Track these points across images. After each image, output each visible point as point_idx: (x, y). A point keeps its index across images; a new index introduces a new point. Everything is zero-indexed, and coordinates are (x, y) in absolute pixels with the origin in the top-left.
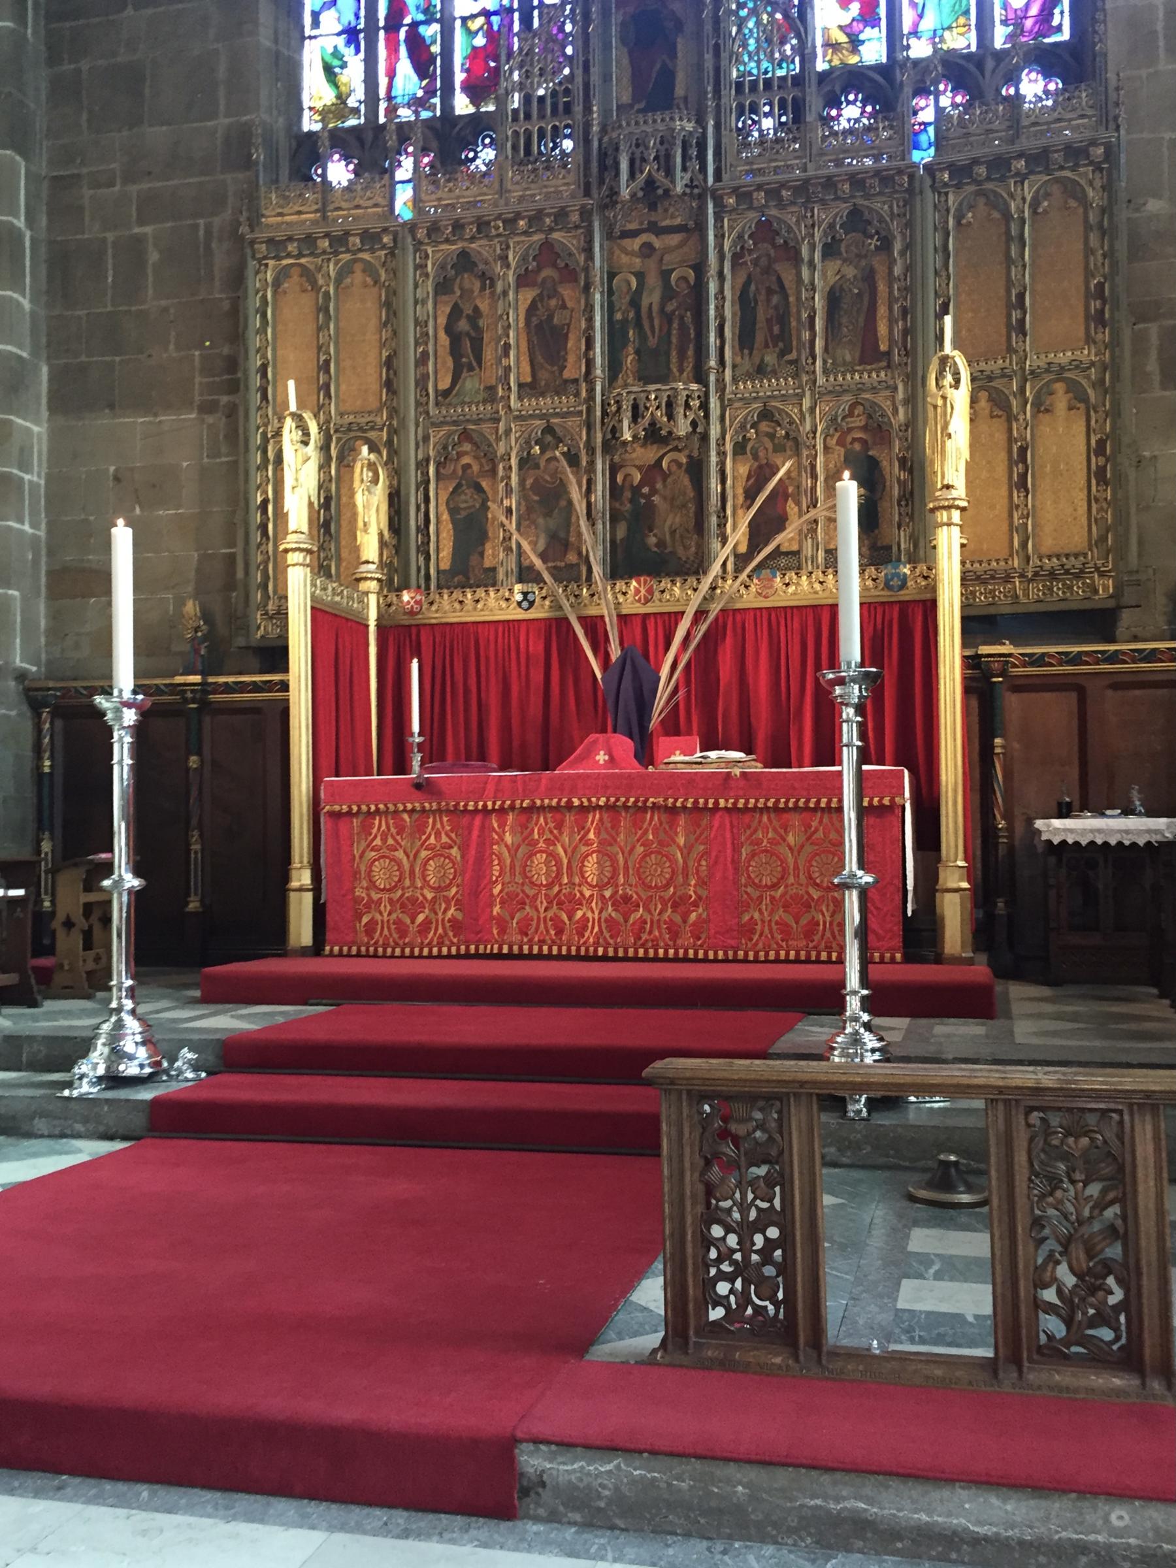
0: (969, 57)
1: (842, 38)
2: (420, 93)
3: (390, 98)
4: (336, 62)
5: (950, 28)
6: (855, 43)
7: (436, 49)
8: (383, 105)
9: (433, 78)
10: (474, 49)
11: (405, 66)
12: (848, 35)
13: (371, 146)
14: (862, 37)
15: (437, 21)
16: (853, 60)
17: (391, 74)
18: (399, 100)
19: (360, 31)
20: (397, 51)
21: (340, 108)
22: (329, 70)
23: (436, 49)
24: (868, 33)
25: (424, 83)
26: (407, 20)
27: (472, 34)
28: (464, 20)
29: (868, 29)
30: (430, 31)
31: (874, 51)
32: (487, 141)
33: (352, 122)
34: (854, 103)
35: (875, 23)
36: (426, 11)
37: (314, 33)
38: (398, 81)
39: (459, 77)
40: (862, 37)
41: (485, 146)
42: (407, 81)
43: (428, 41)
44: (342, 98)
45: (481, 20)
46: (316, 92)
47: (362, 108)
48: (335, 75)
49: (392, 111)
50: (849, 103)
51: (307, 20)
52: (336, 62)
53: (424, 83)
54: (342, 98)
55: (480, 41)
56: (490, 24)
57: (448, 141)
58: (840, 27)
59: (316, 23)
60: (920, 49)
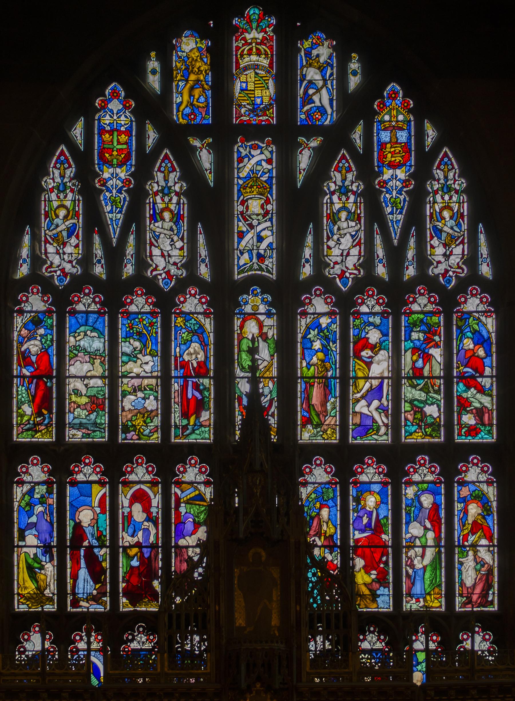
0: (438, 614)
1: (367, 592)
2: (95, 592)
3: (74, 593)
4: (36, 565)
5: (429, 594)
6: (374, 596)
7: (106, 565)
8: (69, 598)
9: (104, 584)
10: (132, 567)
11: (83, 573)
12: (370, 590)
13: (62, 625)
14: (378, 592)
15: (107, 547)
16: (373, 608)
17: (75, 577)
18: (81, 596)
19: (54, 547)
20: (79, 563)
21: (39, 597)
22: (30, 569)
23: (106, 565)
24: (381, 591)
25: (97, 586)
26: (86, 543)
27: (130, 558)
28: (125, 548)
29: (382, 588)
30: (102, 553)
31: (384, 603)
32: (141, 629)
33: (48, 608)
34: (373, 632)
35: (386, 585)
36: (98, 539)
37: (21, 543)
38: (80, 583)
39: (122, 585)
40: (378, 592)
41: (139, 633)
42: (85, 583)
43: (101, 560)
44: (40, 590)
45: (135, 550)
46: (24, 584)
47: (56, 597)
48: (36, 573)
49: (75, 603)
50: (370, 632)
51: (16, 534)
52: (36, 565)
53: (97, 586)
54: (40, 590)
55: (135, 563)
56: (142, 553)
57: (113, 627)
58: (365, 584)
59: (22, 537)
60: (411, 605)
